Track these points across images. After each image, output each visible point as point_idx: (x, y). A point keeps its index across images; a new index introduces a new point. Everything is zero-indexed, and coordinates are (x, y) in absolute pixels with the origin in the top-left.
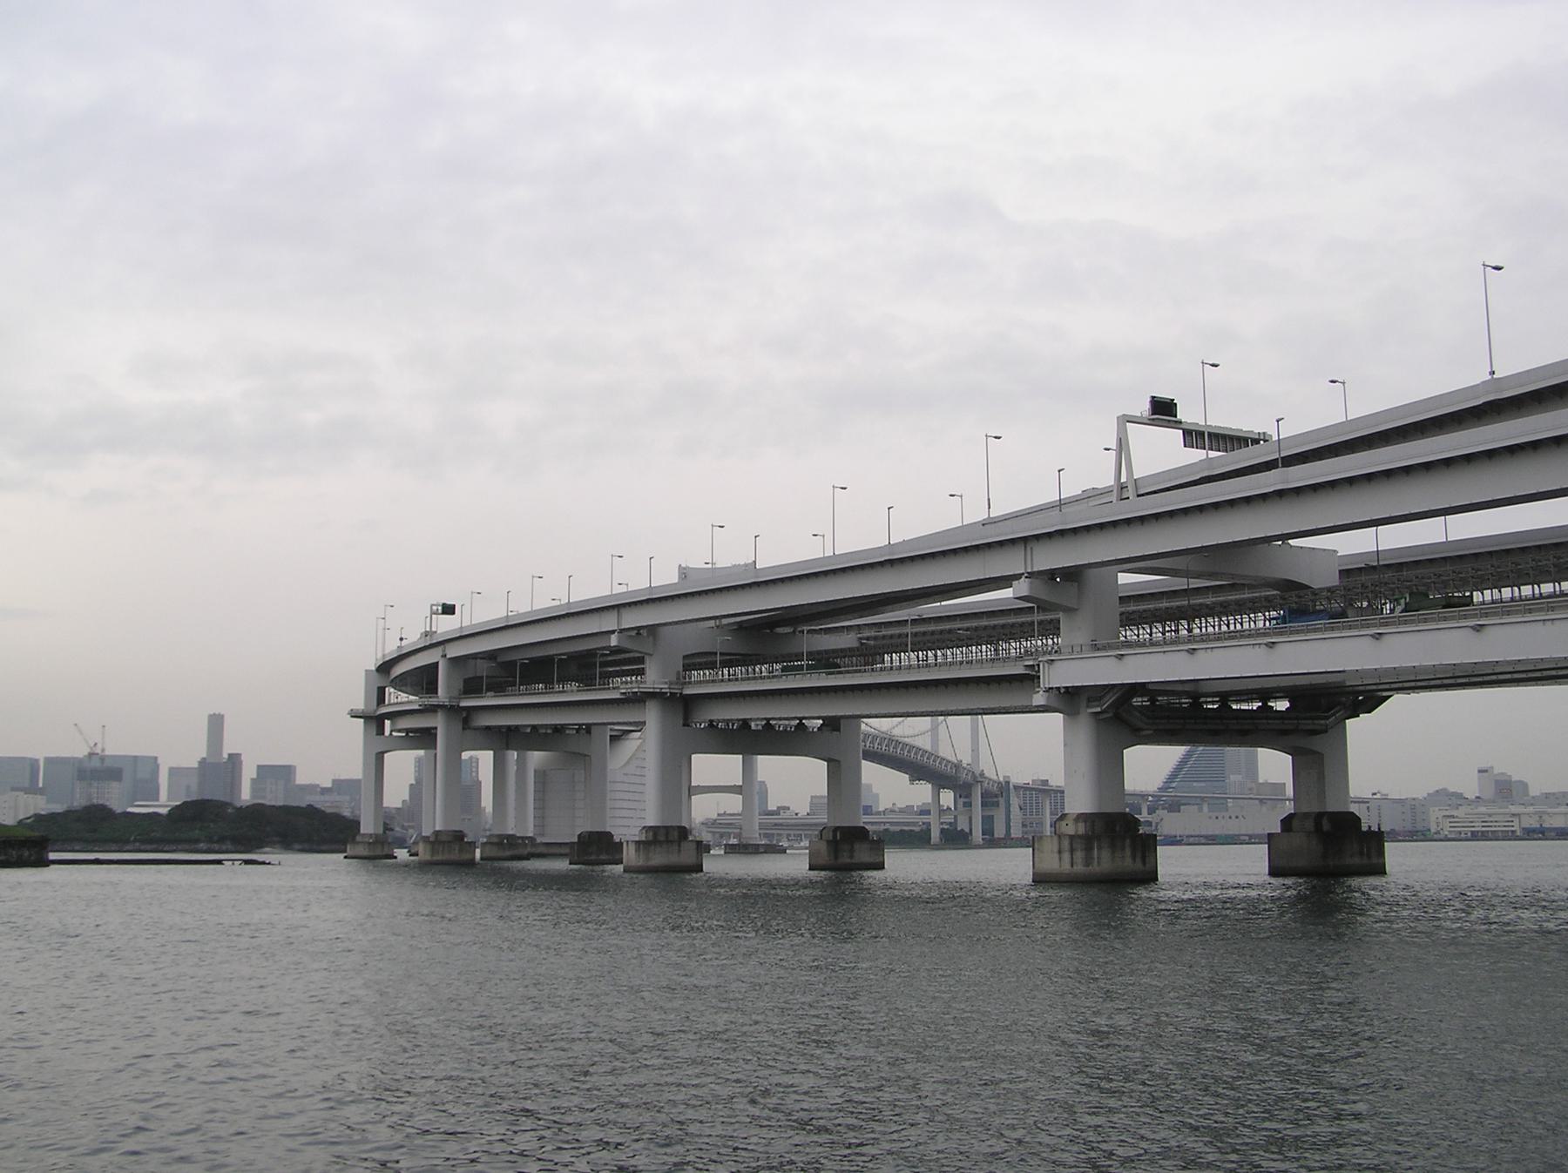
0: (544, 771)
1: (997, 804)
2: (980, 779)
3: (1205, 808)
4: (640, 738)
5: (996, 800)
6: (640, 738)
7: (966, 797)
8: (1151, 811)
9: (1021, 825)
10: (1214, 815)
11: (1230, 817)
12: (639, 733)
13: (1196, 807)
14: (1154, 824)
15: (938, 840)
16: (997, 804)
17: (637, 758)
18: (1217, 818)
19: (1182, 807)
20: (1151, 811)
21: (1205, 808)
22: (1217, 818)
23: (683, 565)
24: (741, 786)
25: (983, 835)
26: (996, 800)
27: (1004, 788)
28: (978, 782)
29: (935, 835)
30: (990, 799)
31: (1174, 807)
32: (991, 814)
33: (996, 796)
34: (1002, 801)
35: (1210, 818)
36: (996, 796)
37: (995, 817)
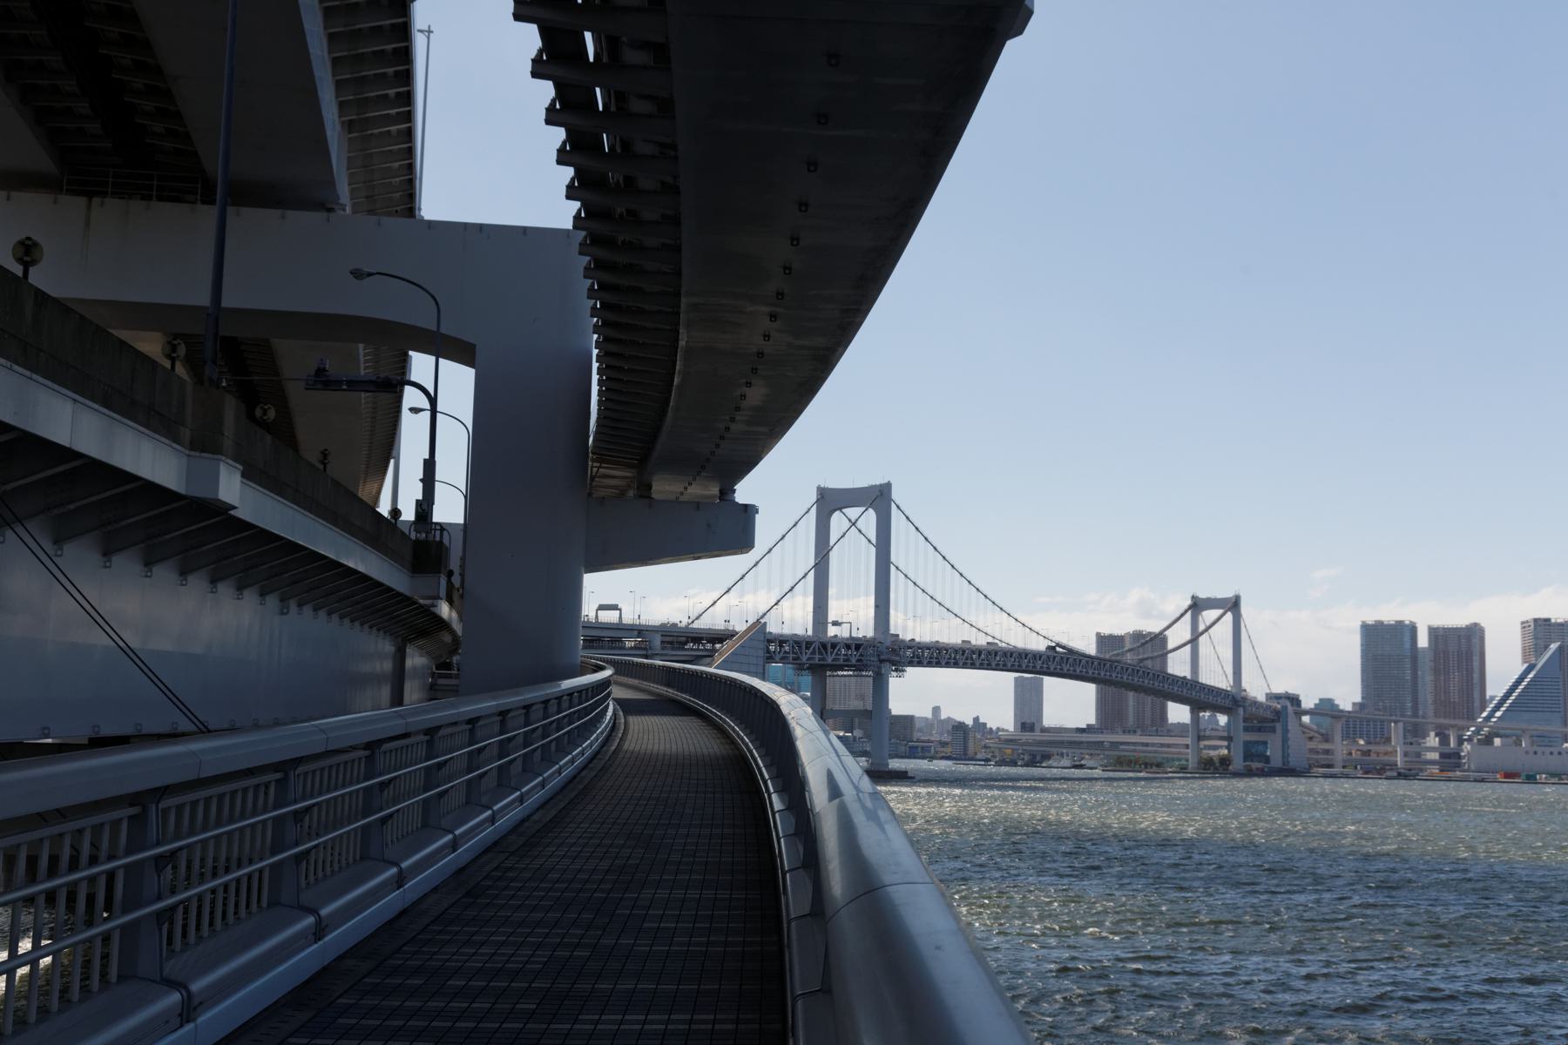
1: (1273, 730)
5: (1272, 725)
10: (1540, 750)
16: (1273, 730)
18: (1543, 753)
22: (1543, 753)
23: (822, 486)
24: (871, 711)
33: (1273, 721)
34: (1278, 726)
36: (1273, 721)
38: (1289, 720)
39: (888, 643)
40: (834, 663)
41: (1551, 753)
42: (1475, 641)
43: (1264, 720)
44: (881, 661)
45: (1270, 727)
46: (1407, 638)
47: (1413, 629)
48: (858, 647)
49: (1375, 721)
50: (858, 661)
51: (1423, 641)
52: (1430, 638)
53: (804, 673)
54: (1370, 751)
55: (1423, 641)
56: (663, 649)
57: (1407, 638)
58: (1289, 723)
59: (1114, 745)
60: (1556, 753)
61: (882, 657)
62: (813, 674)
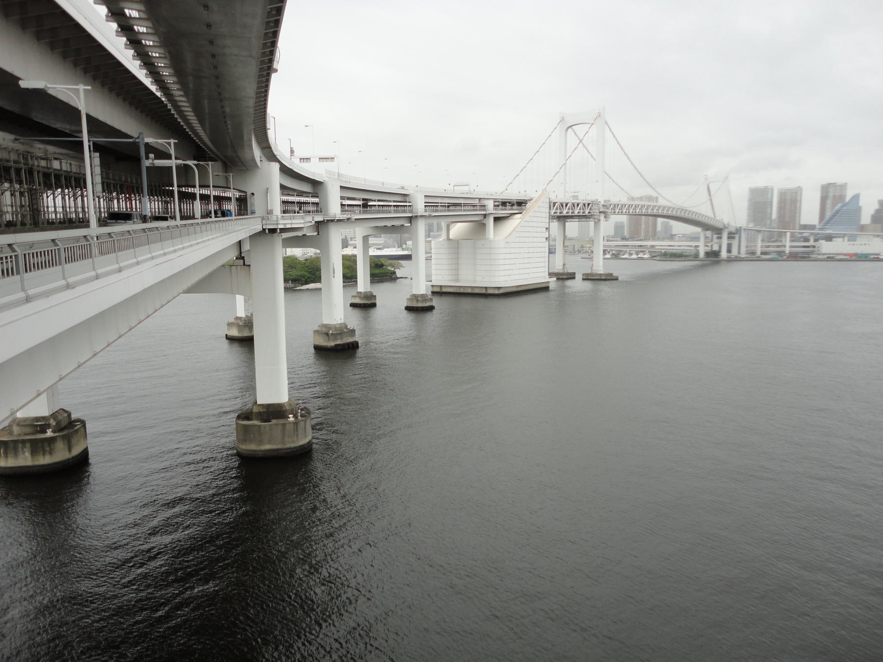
0: (458, 241)
1: (733, 238)
4: (520, 218)
5: (733, 236)
6: (520, 218)
7: (718, 234)
8: (816, 240)
10: (850, 242)
12: (521, 215)
13: (842, 239)
14: (816, 247)
17: (516, 231)
20: (816, 240)
21: (846, 239)
26: (733, 236)
29: (702, 254)
31: (829, 238)
33: (734, 234)
34: (737, 236)
35: (850, 245)
36: (734, 234)
39: (602, 203)
40: (567, 215)
44: (600, 212)
47: (772, 190)
48: (589, 204)
50: (589, 212)
53: (555, 220)
56: (496, 210)
59: (653, 246)
61: (601, 210)
62: (559, 220)
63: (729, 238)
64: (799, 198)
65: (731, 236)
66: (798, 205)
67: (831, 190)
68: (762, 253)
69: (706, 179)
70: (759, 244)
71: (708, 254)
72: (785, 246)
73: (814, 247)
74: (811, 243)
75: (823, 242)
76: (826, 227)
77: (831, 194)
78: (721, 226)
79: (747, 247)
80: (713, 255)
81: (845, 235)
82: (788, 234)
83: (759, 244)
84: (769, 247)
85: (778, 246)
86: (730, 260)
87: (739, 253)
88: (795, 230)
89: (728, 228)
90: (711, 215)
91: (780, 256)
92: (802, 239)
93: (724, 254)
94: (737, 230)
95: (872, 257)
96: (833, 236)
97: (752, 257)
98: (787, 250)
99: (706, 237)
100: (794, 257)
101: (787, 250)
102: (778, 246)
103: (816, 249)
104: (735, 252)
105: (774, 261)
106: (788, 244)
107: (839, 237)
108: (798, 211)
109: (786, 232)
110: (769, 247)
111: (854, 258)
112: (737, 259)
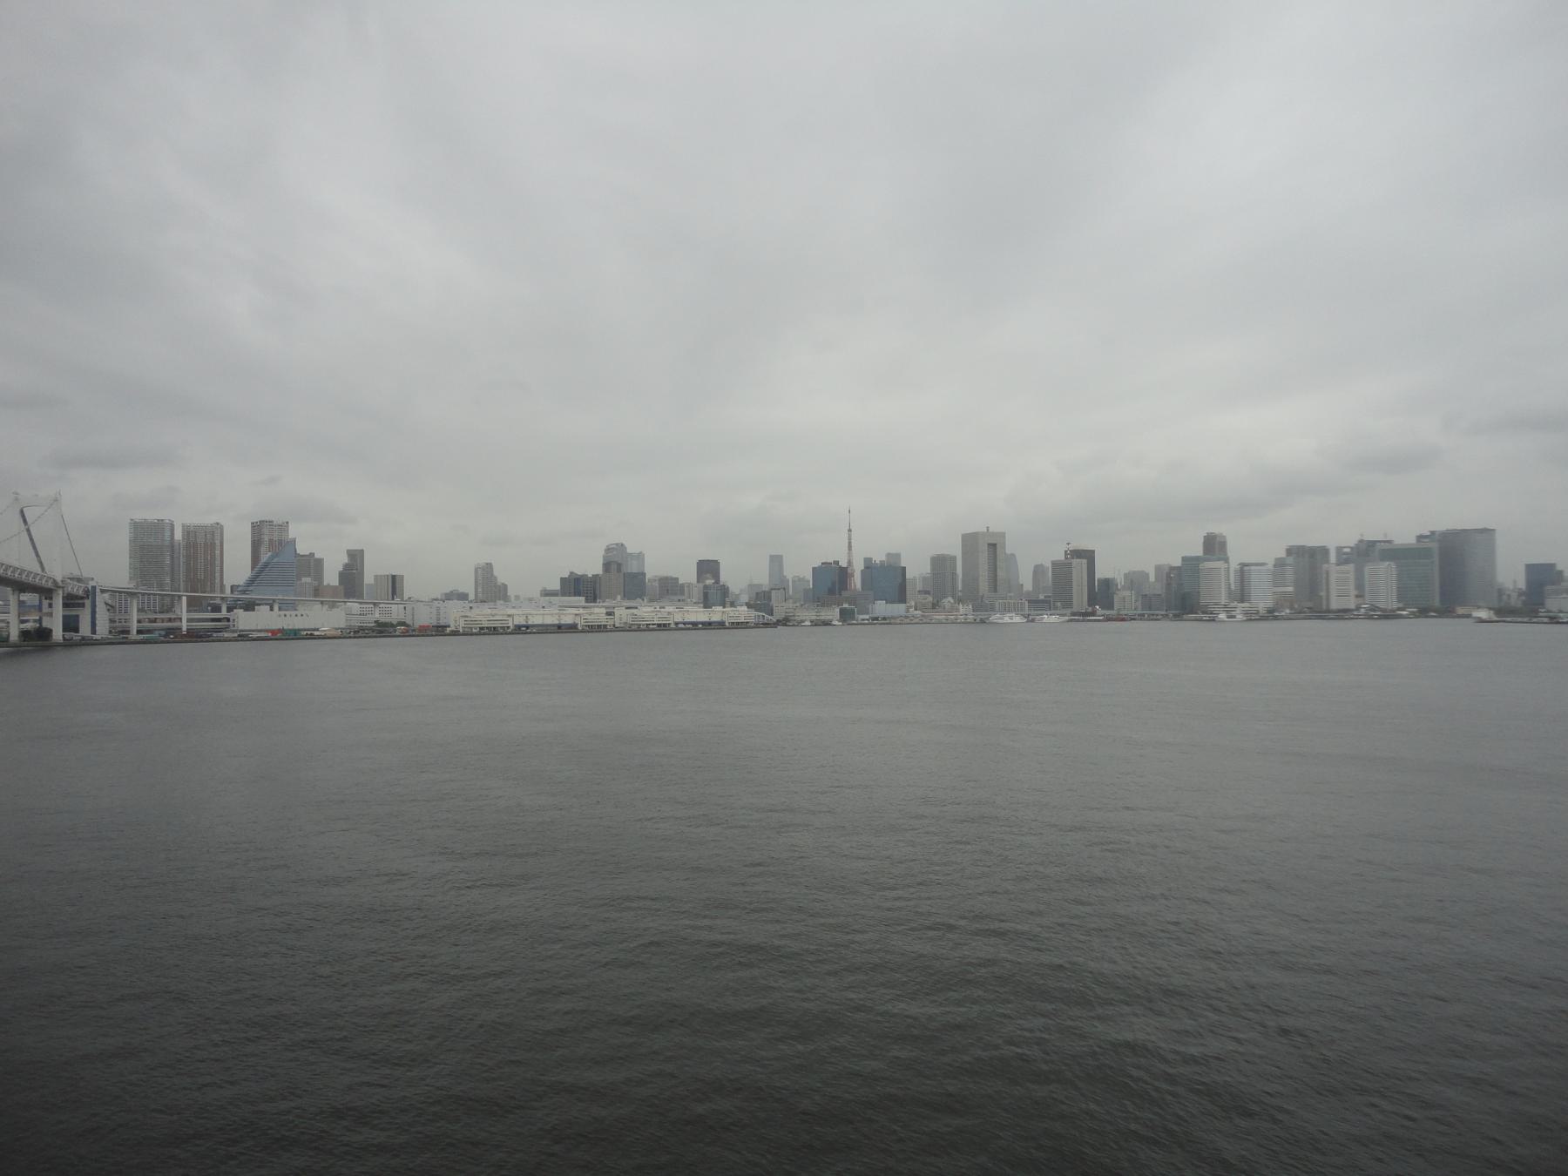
2: (60, 584)
3: (276, 607)
5: (81, 601)
8: (230, 609)
9: (108, 622)
10: (282, 613)
11: (296, 615)
15: (16, 638)
16: (83, 605)
18: (285, 615)
19: (256, 607)
20: (230, 609)
25: (64, 630)
26: (81, 601)
27: (90, 593)
28: (60, 587)
29: (14, 635)
30: (71, 601)
31: (249, 606)
32: (74, 613)
34: (88, 603)
35: (280, 616)
36: (82, 598)
37: (81, 616)
38: (97, 597)
41: (296, 615)
42: (217, 537)
43: (77, 597)
45: (79, 604)
46: (167, 534)
47: (172, 526)
49: (149, 594)
51: (178, 535)
52: (183, 535)
54: (156, 619)
55: (178, 535)
57: (167, 534)
58: (97, 599)
60: (299, 615)
63: (65, 605)
64: (218, 542)
65: (71, 601)
66: (218, 552)
67: (266, 530)
68: (139, 632)
69: (17, 499)
70: (135, 616)
71: (25, 634)
72: (181, 619)
73: (228, 620)
74: (224, 613)
75: (239, 612)
76: (251, 588)
77: (266, 538)
78: (50, 585)
79: (112, 621)
80: (38, 638)
81: (274, 600)
82: (184, 599)
83: (135, 616)
84: (155, 621)
85: (170, 620)
86: (68, 644)
87: (94, 631)
88: (179, 591)
89: (63, 587)
90: (36, 568)
91: (173, 635)
92: (209, 608)
93: (58, 634)
94: (87, 591)
95: (305, 633)
96: (257, 602)
97: (120, 636)
98: (184, 626)
99: (21, 604)
100: (195, 636)
101: (184, 626)
102: (170, 620)
103: (231, 623)
104: (85, 629)
105: (150, 643)
106: (185, 617)
107: (266, 604)
108: (218, 562)
109: (180, 597)
110: (155, 621)
111: (279, 635)
112: (86, 642)
